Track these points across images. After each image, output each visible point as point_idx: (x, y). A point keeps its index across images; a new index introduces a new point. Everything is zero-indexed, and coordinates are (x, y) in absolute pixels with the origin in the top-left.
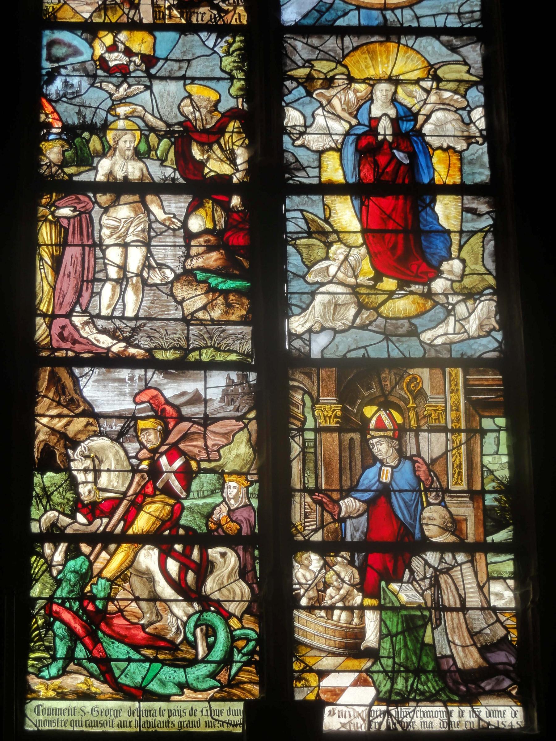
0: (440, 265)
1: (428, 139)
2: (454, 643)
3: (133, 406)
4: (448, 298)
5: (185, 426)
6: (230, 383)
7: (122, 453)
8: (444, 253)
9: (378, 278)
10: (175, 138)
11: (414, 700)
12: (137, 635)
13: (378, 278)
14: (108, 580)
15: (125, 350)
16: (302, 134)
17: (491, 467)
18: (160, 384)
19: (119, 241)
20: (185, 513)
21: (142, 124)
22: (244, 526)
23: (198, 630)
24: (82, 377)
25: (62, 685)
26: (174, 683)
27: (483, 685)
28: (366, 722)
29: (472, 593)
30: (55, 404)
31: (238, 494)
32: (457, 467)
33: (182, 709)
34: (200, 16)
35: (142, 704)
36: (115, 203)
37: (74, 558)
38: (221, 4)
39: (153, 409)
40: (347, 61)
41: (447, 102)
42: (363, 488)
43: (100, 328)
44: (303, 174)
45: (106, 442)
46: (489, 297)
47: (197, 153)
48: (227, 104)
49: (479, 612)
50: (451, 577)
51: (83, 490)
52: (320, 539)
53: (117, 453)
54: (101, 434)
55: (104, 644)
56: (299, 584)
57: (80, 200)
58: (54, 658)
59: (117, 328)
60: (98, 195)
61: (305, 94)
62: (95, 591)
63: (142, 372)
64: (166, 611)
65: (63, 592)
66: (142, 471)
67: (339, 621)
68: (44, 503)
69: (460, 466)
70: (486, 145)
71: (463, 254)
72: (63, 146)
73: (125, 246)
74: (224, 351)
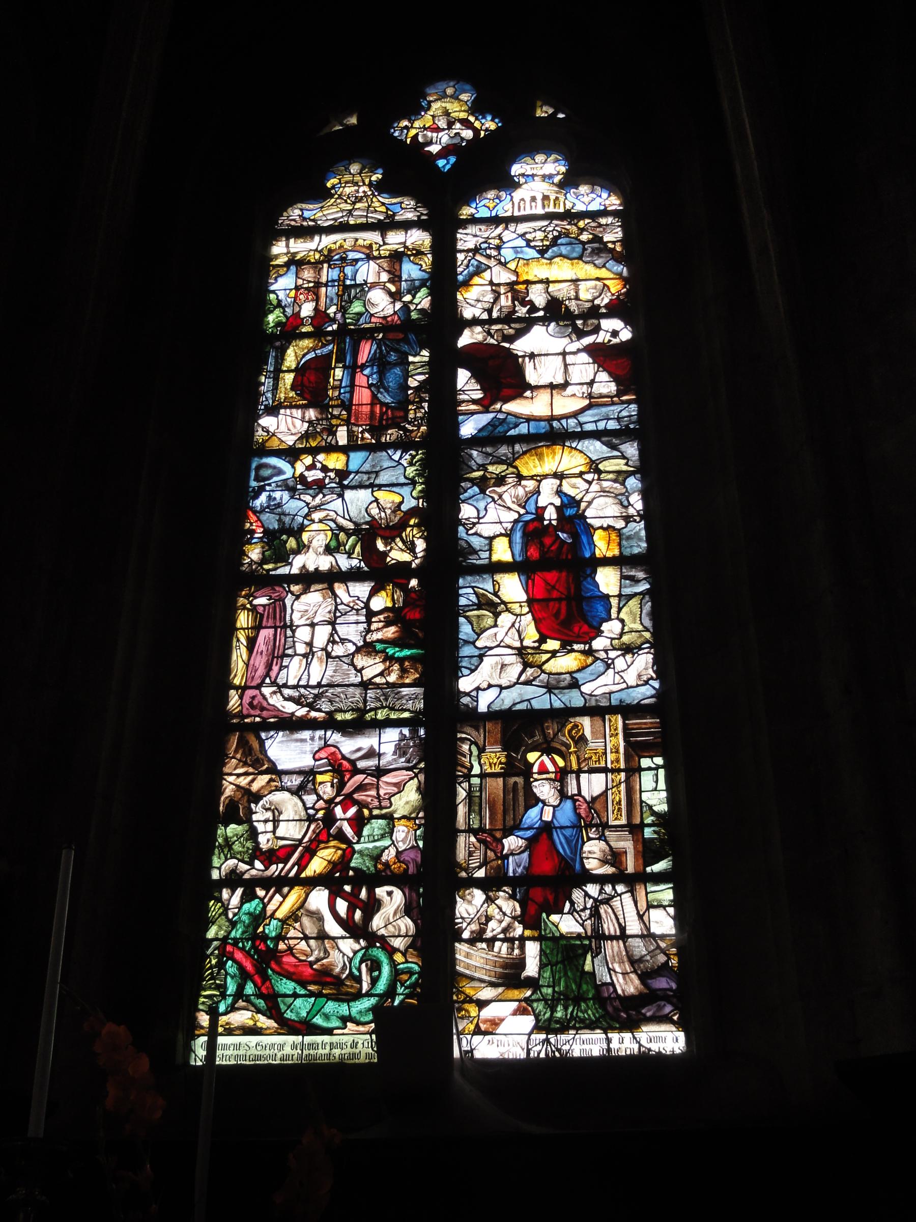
0: (601, 626)
1: (589, 521)
2: (615, 971)
3: (312, 762)
4: (607, 654)
5: (359, 778)
6: (403, 738)
7: (300, 804)
8: (604, 615)
9: (542, 640)
10: (362, 535)
11: (574, 1028)
12: (303, 972)
13: (542, 640)
14: (280, 920)
15: (307, 714)
16: (474, 524)
17: (649, 802)
18: (338, 742)
19: (308, 622)
20: (356, 856)
21: (333, 525)
22: (411, 866)
23: (364, 965)
24: (267, 739)
25: (230, 1021)
26: (338, 1017)
27: (643, 1011)
28: (525, 1050)
29: (632, 921)
30: (241, 764)
31: (406, 837)
32: (617, 804)
33: (344, 1042)
34: (388, 436)
35: (305, 1037)
36: (306, 591)
37: (249, 901)
38: (407, 426)
39: (330, 764)
40: (517, 463)
41: (607, 489)
42: (526, 826)
43: (286, 696)
44: (476, 556)
45: (286, 795)
46: (646, 651)
47: (380, 545)
48: (410, 503)
49: (638, 940)
50: (611, 907)
51: (262, 839)
52: (483, 875)
53: (296, 805)
54: (282, 789)
55: (273, 981)
56: (462, 918)
57: (275, 590)
58: (223, 996)
59: (302, 695)
60: (292, 586)
61: (479, 492)
62: (267, 931)
63: (322, 732)
64: (333, 948)
65: (236, 933)
66: (318, 819)
67: (499, 952)
68: (226, 852)
69: (619, 803)
70: (643, 522)
71: (622, 615)
72: (263, 547)
73: (313, 625)
74: (398, 710)
